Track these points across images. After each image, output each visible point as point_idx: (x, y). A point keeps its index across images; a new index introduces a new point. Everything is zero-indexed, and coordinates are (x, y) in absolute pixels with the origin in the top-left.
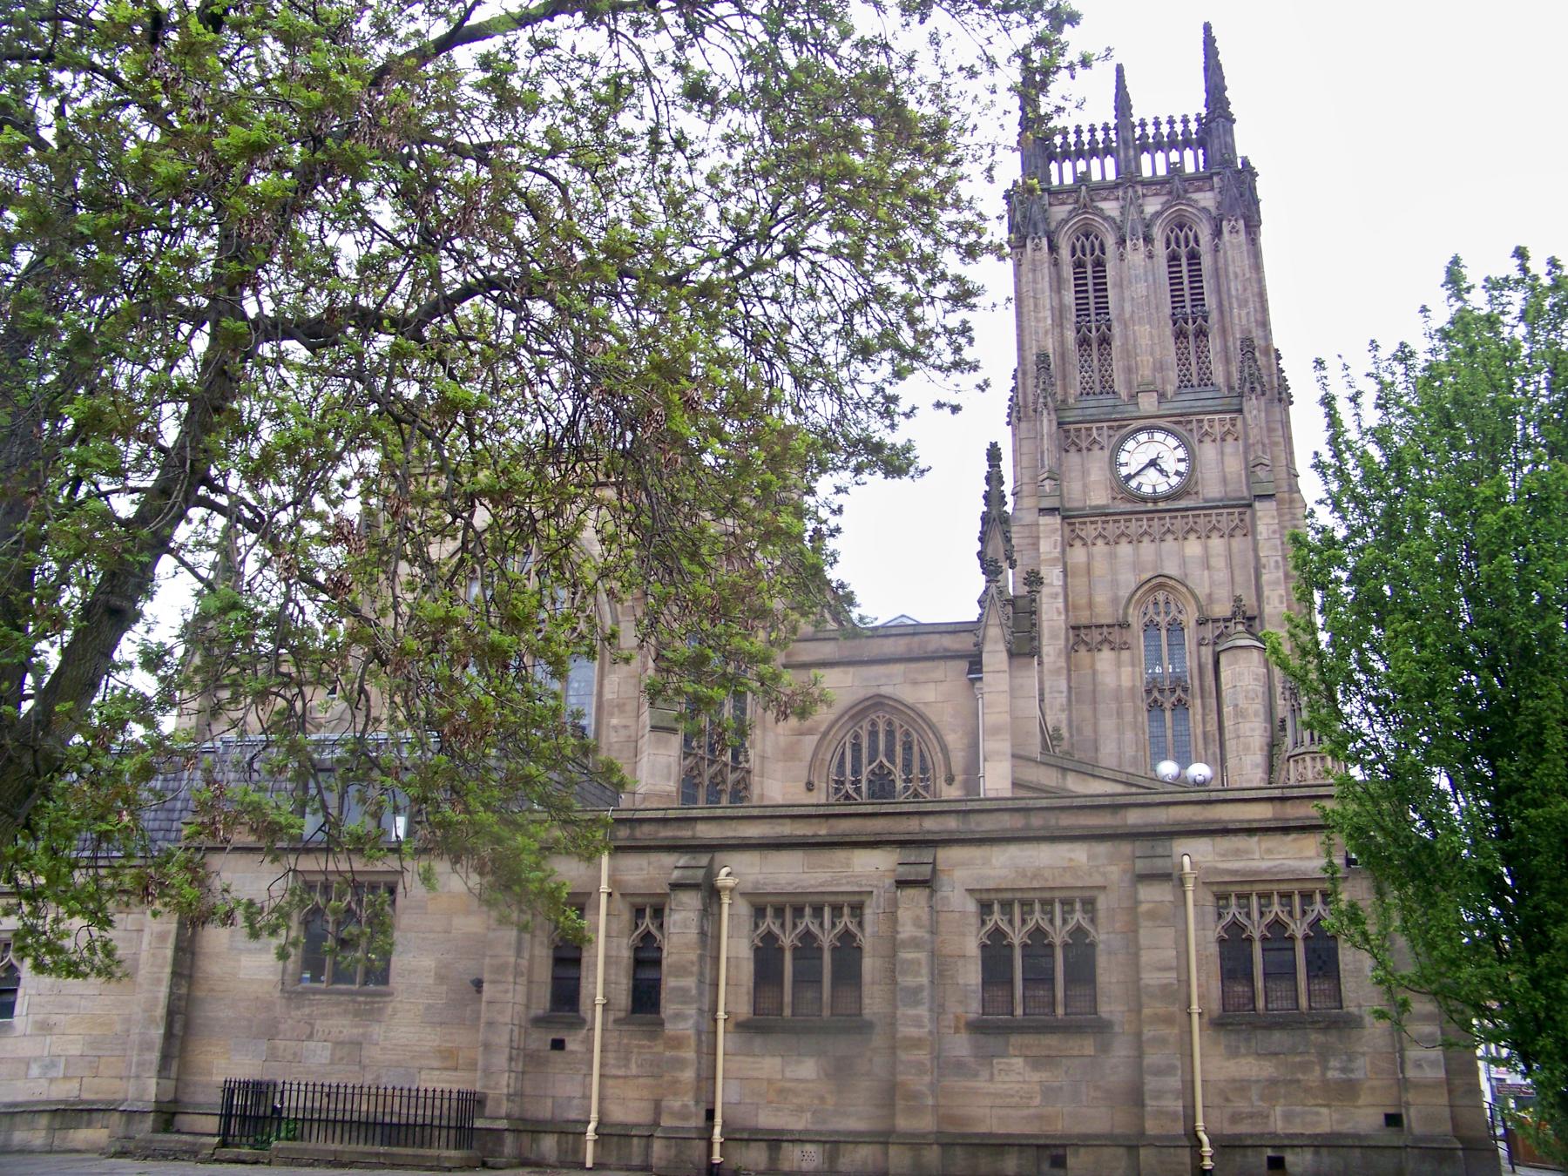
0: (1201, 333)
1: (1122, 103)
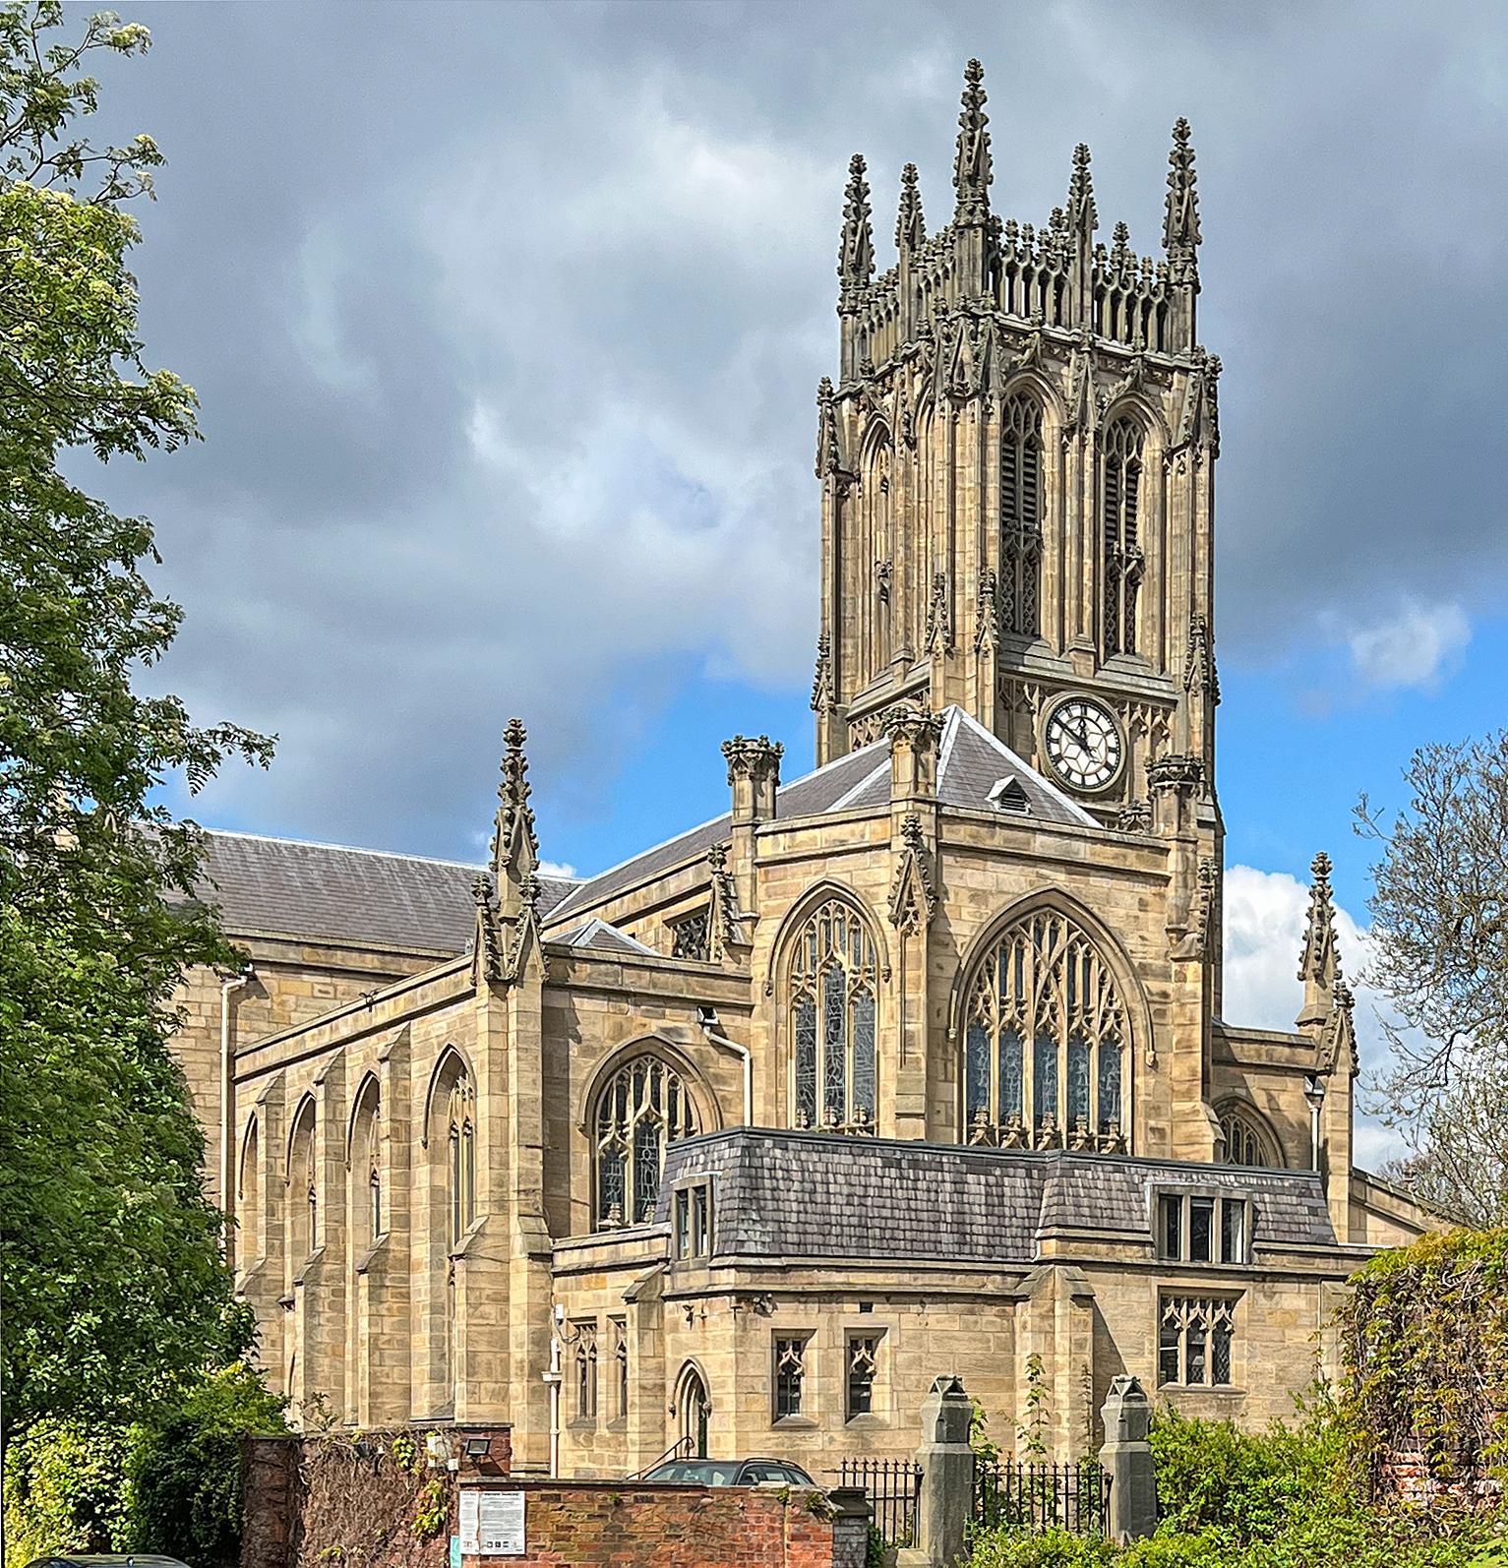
1: (1082, 219)
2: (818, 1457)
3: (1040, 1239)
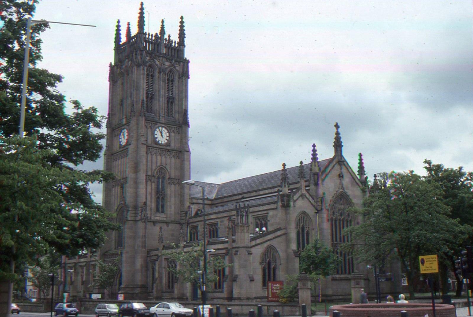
0: (172, 103)
1: (163, 31)
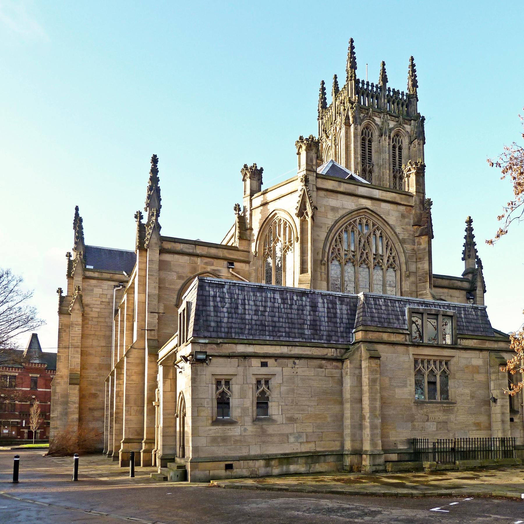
2: (238, 438)
3: (355, 333)
